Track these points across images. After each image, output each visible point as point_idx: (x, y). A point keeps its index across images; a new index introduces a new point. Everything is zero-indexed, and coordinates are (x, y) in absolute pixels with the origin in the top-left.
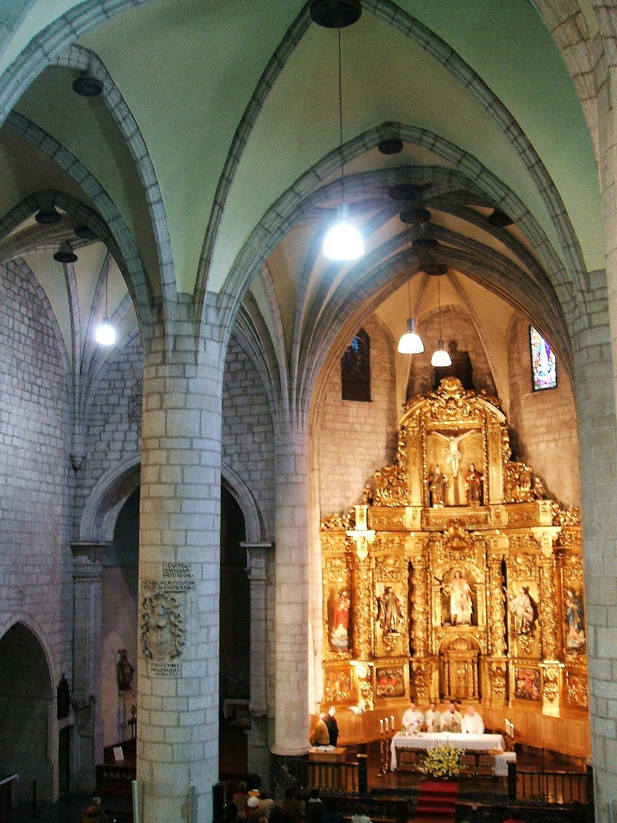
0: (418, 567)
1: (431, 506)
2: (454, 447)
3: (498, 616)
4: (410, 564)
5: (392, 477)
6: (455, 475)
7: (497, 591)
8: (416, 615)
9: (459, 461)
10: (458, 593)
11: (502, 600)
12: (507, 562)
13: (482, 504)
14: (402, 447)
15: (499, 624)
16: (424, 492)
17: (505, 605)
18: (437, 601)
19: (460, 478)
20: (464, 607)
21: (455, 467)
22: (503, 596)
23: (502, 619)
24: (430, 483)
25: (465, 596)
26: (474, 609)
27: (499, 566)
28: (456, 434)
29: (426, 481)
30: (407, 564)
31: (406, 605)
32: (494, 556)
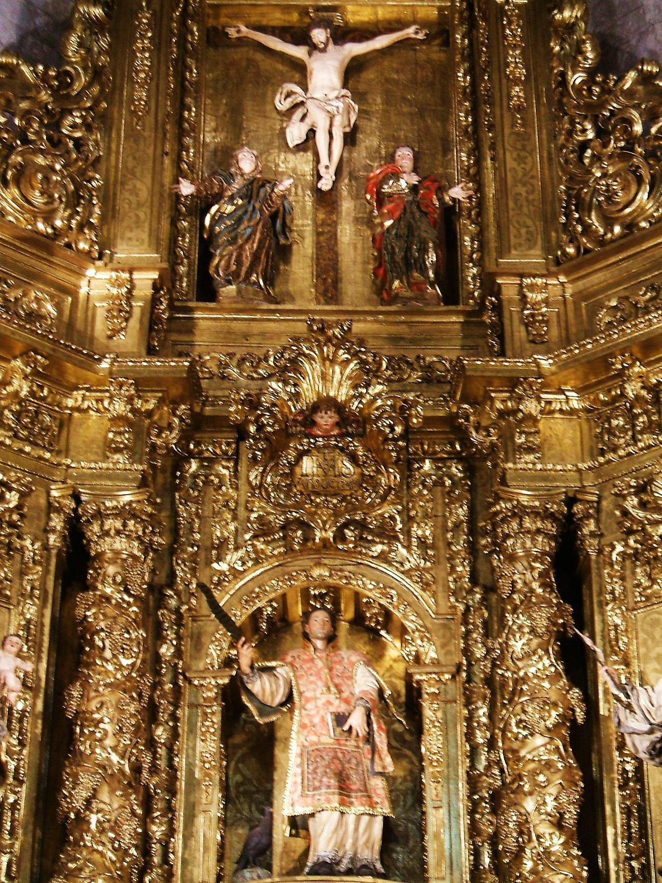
0: (115, 545)
1: (207, 291)
2: (326, 72)
3: (544, 803)
4: (75, 529)
5: (24, 105)
6: (325, 184)
7: (540, 667)
8: (86, 780)
9: (350, 139)
10: (321, 700)
11: (568, 718)
12: (591, 526)
13: (452, 292)
14: (93, 25)
15: (556, 842)
16: (175, 233)
17: (584, 738)
18: (203, 748)
19: (347, 205)
20: (355, 783)
21: (331, 151)
22: (576, 693)
23: (571, 817)
24: (200, 205)
25: (357, 720)
26: (409, 796)
27: (542, 544)
28: (343, 34)
29: (187, 188)
30: (57, 522)
31: (35, 728)
32: (525, 497)
